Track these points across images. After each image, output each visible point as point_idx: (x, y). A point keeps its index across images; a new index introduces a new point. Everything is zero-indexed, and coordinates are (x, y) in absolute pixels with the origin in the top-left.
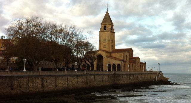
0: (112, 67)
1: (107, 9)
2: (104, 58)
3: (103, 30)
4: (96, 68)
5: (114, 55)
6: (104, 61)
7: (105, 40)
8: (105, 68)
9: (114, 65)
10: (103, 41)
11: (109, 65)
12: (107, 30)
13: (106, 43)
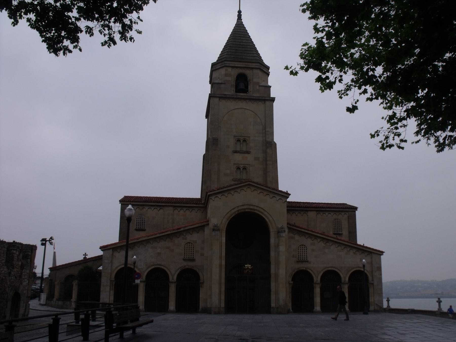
0: (317, 291)
1: (240, 12)
9: (331, 276)
11: (301, 281)
13: (250, 158)
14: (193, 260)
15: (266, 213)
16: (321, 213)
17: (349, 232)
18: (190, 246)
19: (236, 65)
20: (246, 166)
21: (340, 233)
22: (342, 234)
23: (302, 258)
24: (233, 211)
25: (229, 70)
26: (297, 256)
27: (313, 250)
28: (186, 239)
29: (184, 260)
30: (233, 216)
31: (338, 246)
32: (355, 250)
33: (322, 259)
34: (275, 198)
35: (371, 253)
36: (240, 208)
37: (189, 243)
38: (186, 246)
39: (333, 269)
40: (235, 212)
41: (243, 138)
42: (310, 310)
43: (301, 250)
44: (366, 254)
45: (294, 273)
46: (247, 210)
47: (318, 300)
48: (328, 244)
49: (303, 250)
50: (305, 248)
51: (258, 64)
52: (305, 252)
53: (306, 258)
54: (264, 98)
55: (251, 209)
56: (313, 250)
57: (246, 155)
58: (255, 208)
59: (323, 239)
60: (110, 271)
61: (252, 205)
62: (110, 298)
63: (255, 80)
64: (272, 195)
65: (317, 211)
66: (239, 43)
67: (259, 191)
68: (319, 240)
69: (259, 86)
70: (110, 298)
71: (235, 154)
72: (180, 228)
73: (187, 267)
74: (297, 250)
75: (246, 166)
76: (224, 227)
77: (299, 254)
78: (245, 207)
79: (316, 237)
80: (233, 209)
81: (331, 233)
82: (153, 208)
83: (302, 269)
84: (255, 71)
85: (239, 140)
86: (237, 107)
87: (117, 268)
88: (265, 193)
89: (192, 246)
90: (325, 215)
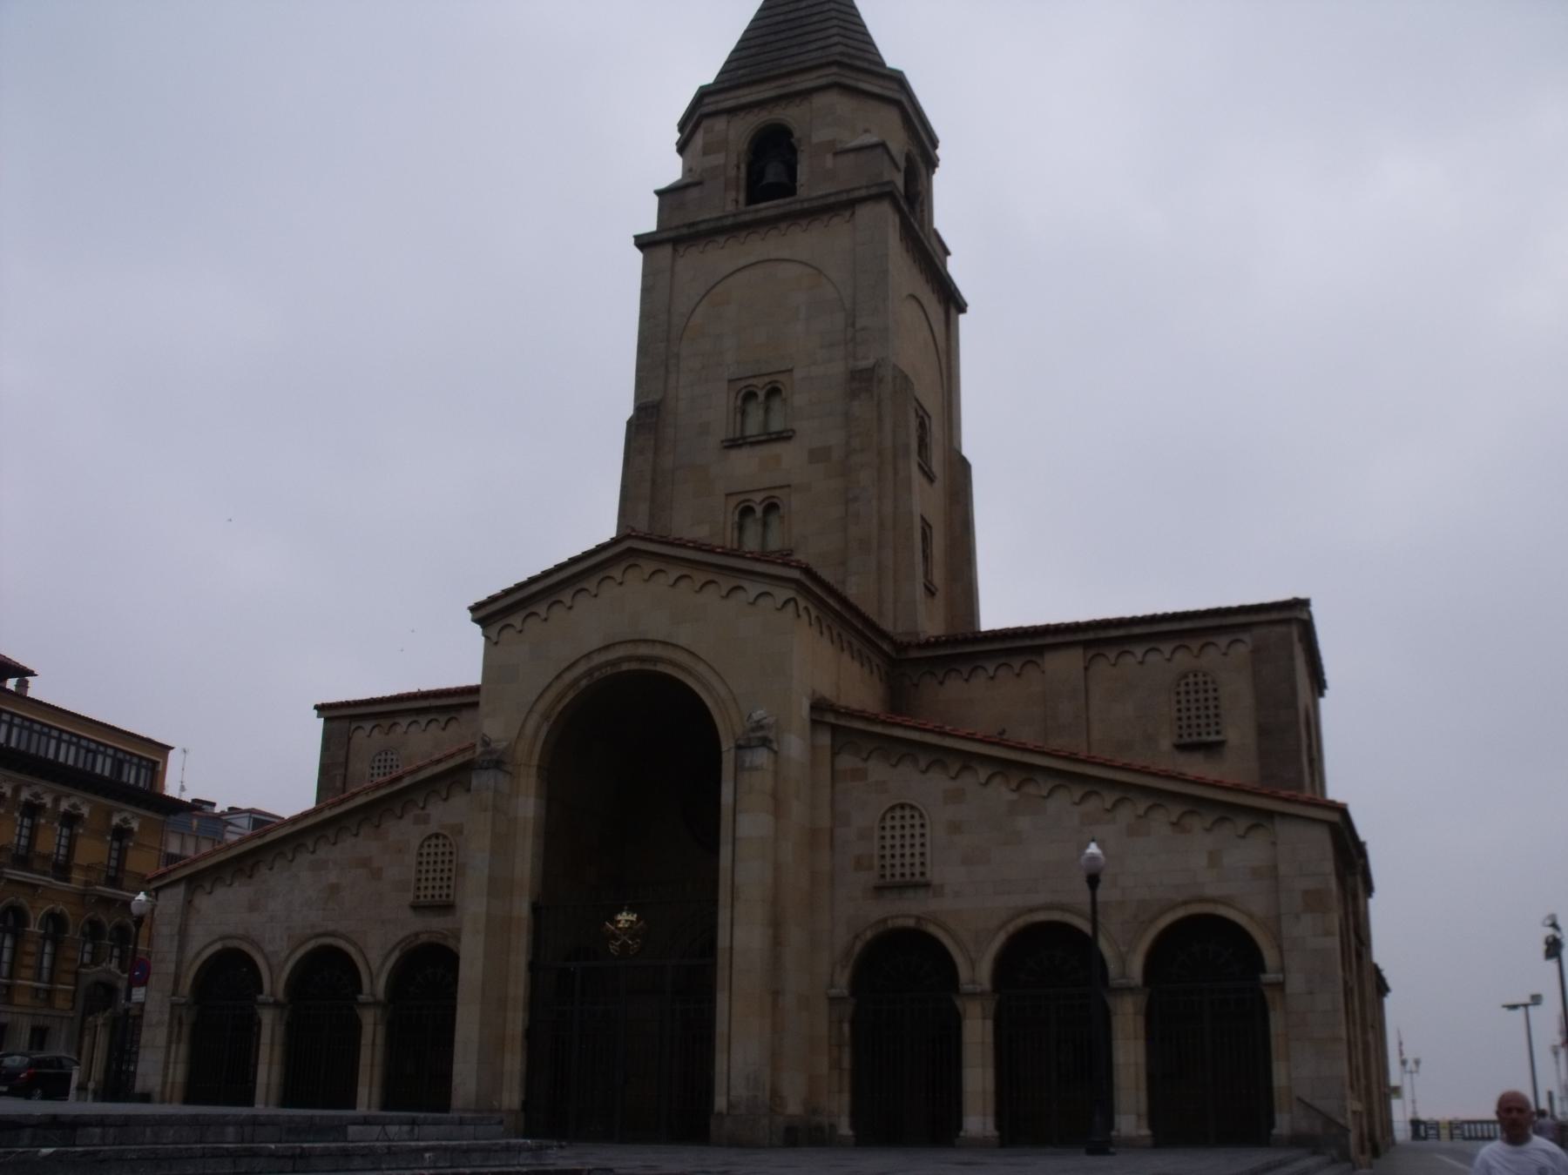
0: (977, 1032)
2: (761, 738)
3: (725, 202)
4: (514, 1063)
5: (981, 702)
6: (756, 837)
7: (761, 392)
8: (771, 1029)
10: (718, 410)
11: (898, 980)
12: (811, 182)
13: (790, 457)
14: (447, 907)
15: (701, 668)
16: (1112, 654)
17: (1263, 731)
18: (441, 849)
19: (743, 101)
20: (777, 493)
21: (1213, 738)
22: (1221, 744)
23: (898, 870)
24: (569, 677)
25: (720, 124)
26: (876, 862)
27: (955, 828)
28: (426, 820)
29: (416, 907)
30: (567, 700)
31: (1083, 798)
32: (1176, 811)
33: (996, 867)
34: (740, 595)
35: (1270, 815)
36: (597, 660)
37: (437, 836)
38: (425, 851)
39: (1056, 916)
40: (577, 681)
41: (767, 379)
42: (941, 1127)
43: (898, 833)
44: (1242, 823)
45: (859, 946)
46: (625, 667)
47: (978, 1078)
48: (1030, 789)
49: (907, 832)
50: (917, 822)
51: (834, 69)
52: (917, 841)
53: (917, 870)
54: (844, 197)
55: (641, 659)
56: (955, 828)
57: (777, 448)
58: (658, 651)
59: (1004, 767)
60: (172, 968)
61: (646, 641)
62: (165, 1075)
63: (821, 135)
64: (726, 583)
65: (1087, 645)
66: (781, 18)
67: (674, 573)
68: (983, 774)
69: (836, 154)
70: (165, 1075)
71: (734, 453)
72: (399, 779)
73: (424, 938)
74: (877, 834)
75: (777, 493)
76: (529, 755)
77: (888, 852)
78: (620, 652)
79: (968, 760)
80: (569, 668)
81: (1166, 744)
82: (423, 720)
83: (900, 922)
84: (820, 100)
85: (750, 396)
86: (742, 262)
87: (198, 954)
88: (700, 577)
89: (447, 850)
90: (1128, 659)
